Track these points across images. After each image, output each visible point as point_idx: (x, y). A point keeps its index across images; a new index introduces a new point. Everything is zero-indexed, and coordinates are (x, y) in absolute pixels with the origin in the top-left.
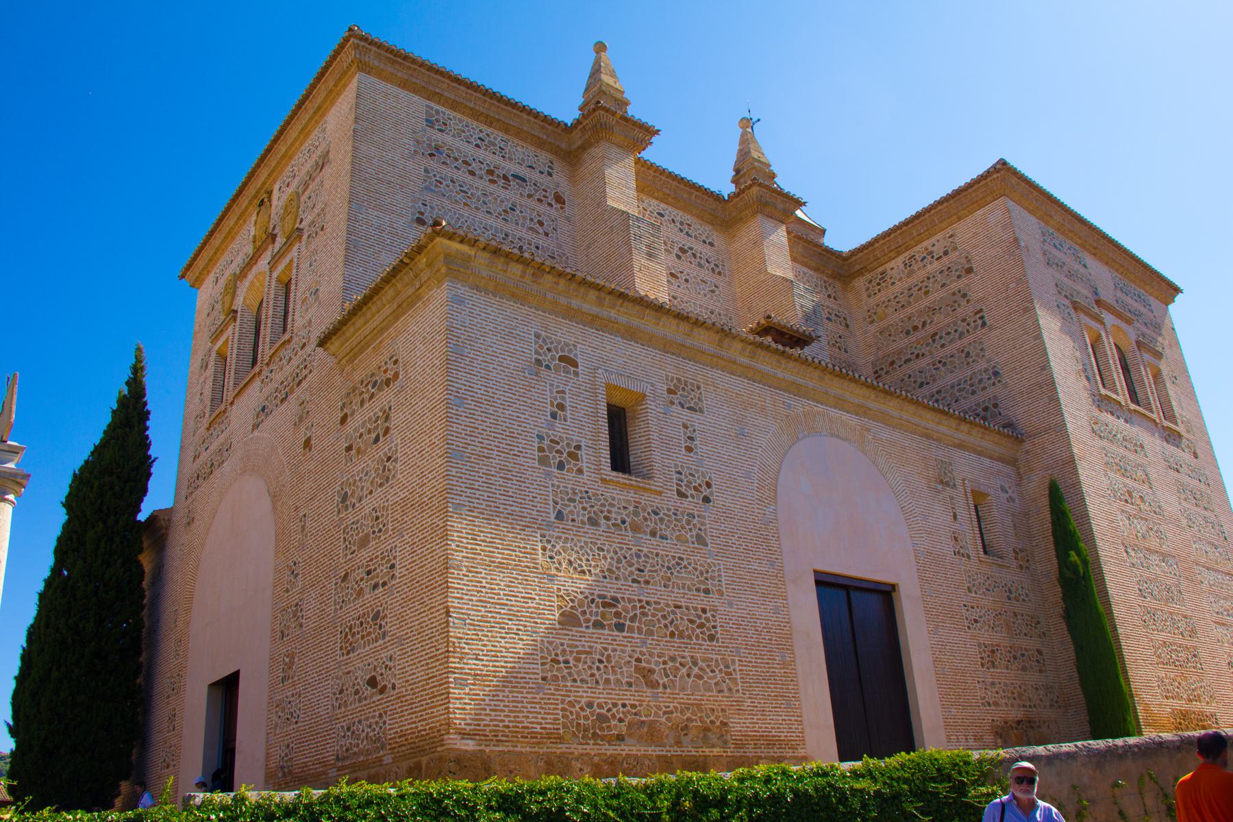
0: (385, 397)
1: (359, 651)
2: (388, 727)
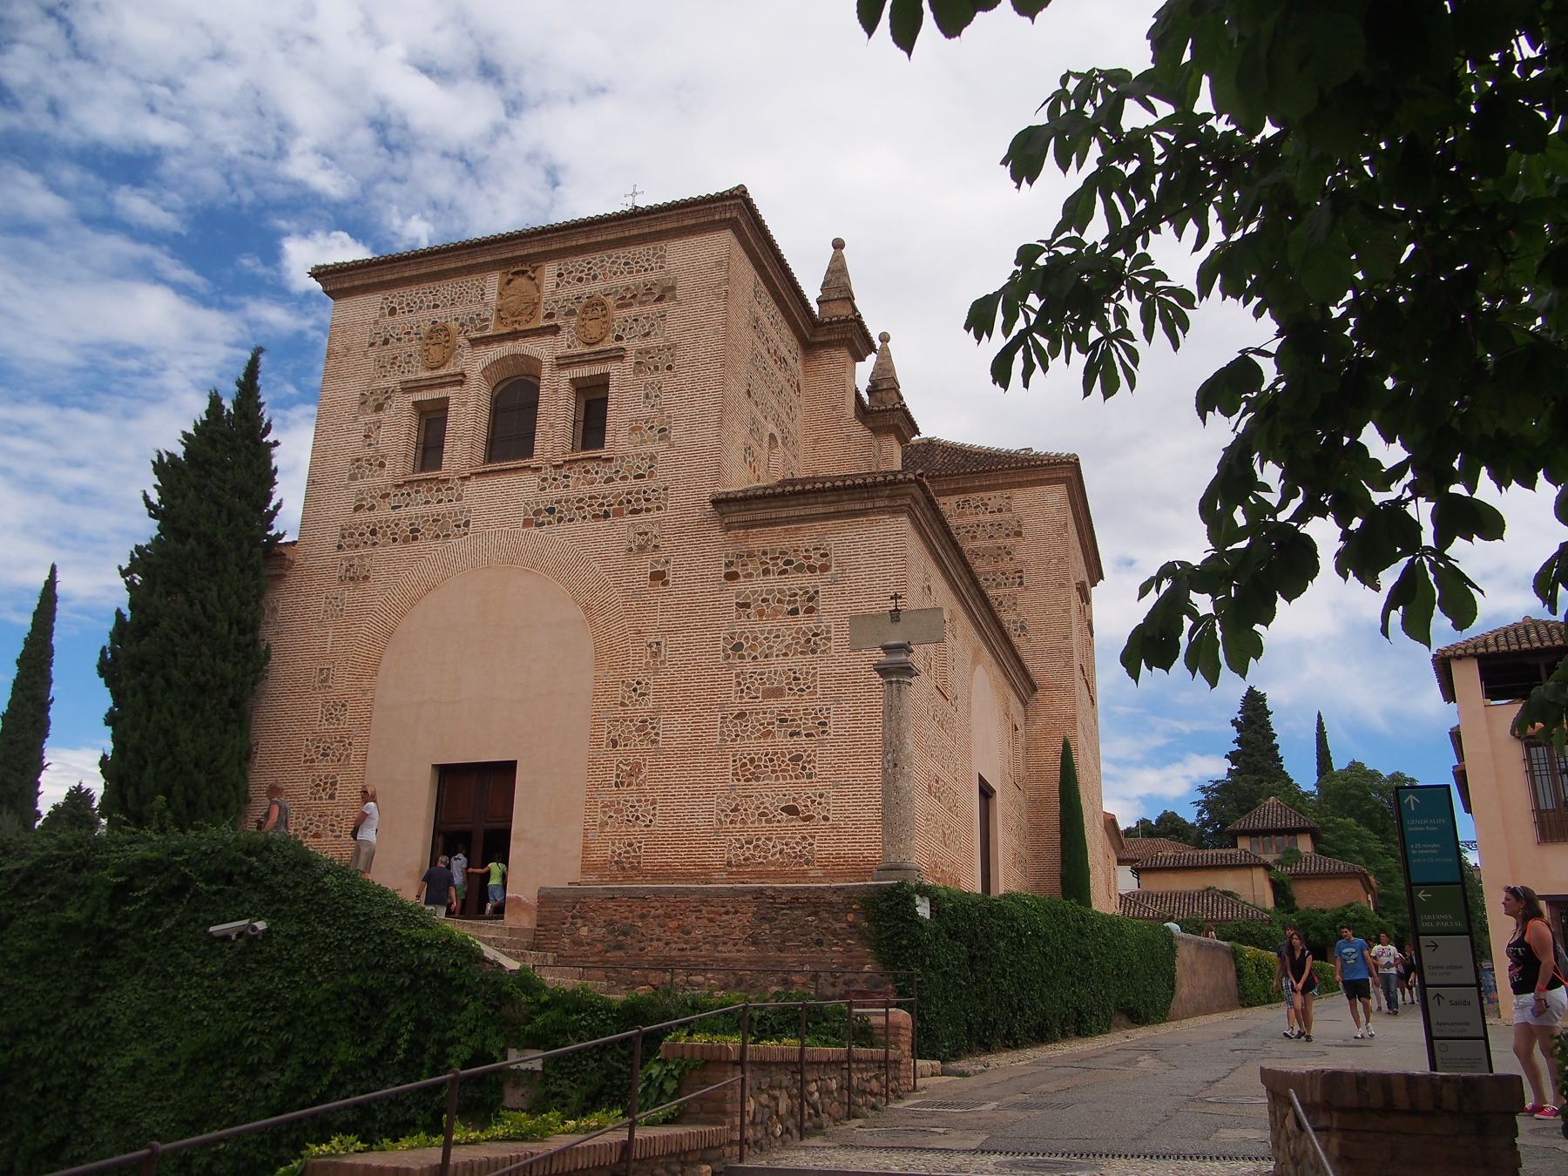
0: (806, 580)
1: (766, 782)
2: (816, 849)
